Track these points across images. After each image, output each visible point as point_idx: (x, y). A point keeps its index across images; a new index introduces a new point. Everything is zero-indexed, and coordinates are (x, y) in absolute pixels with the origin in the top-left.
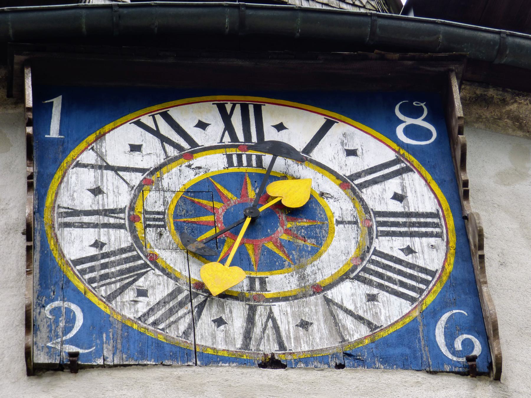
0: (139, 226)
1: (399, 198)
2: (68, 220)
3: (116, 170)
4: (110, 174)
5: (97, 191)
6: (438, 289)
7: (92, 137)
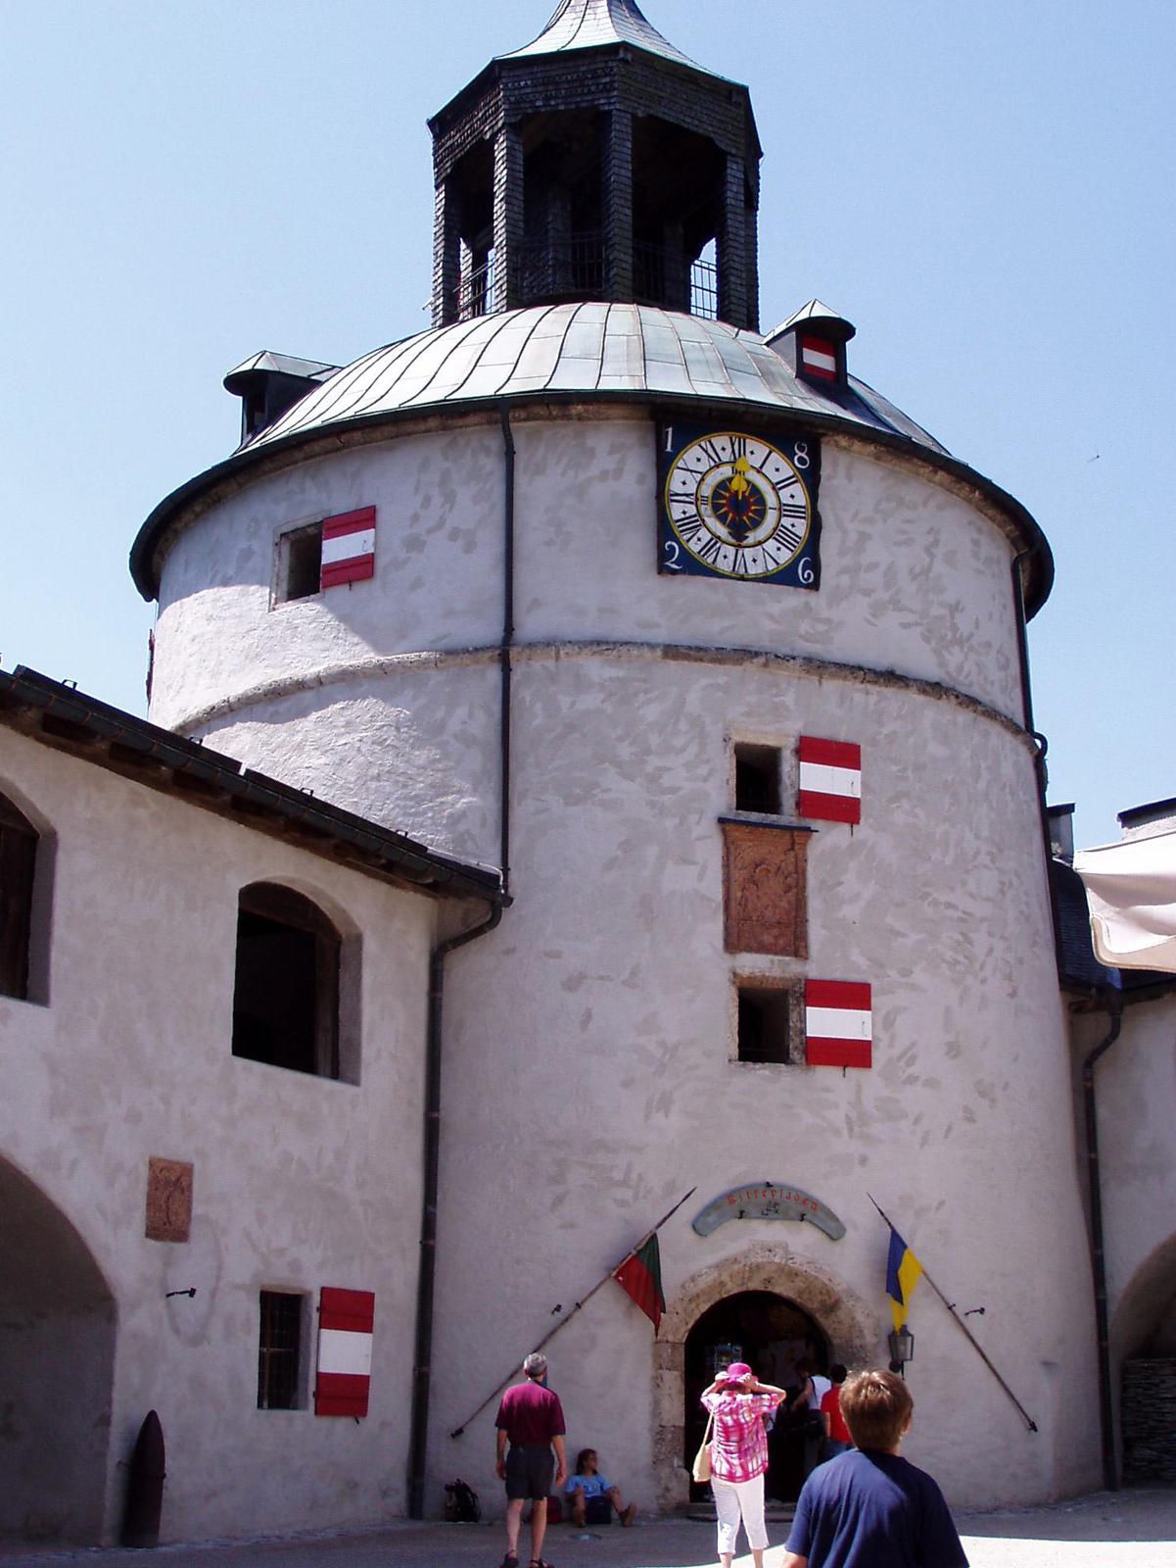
0: (699, 503)
2: (673, 498)
4: (689, 473)
6: (802, 546)
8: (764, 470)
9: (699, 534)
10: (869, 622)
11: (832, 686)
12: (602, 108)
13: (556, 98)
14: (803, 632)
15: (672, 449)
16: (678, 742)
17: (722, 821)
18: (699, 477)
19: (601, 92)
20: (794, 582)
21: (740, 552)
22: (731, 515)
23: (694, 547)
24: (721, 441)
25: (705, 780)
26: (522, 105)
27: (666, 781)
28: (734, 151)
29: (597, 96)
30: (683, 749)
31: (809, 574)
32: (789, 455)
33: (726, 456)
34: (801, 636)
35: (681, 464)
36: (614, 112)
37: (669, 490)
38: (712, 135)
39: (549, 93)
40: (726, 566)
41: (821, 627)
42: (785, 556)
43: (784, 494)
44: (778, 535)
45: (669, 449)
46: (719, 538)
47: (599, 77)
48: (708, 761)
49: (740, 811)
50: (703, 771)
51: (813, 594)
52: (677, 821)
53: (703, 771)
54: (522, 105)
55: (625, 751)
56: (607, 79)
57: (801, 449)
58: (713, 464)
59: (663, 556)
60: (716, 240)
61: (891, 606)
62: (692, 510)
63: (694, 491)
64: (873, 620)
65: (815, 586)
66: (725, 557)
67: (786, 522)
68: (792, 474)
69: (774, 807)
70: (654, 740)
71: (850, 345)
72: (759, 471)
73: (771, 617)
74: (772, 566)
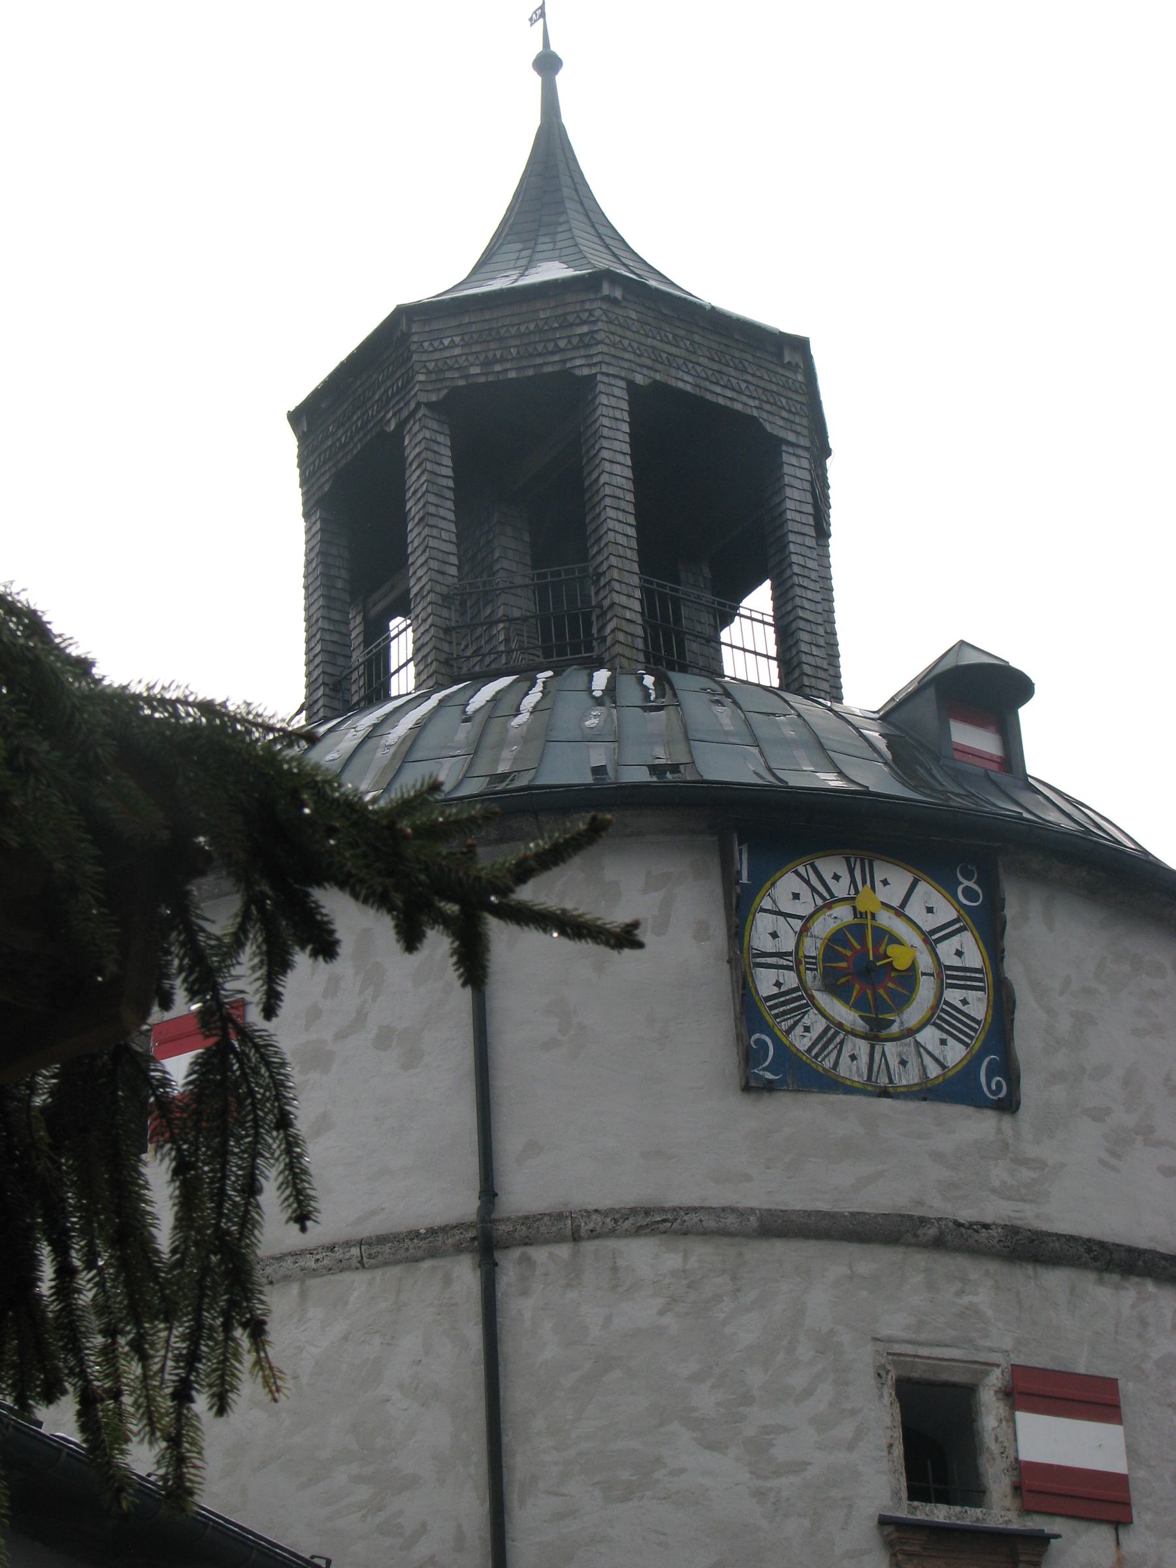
0: (802, 968)
1: (959, 953)
2: (759, 960)
3: (786, 915)
4: (781, 918)
5: (774, 935)
6: (982, 1037)
7: (768, 884)
8: (908, 911)
9: (806, 1021)
10: (1102, 1162)
11: (1056, 1279)
12: (578, 372)
13: (502, 360)
14: (997, 1183)
15: (749, 878)
16: (798, 1379)
17: (884, 1521)
18: (798, 924)
19: (575, 348)
20: (977, 1101)
21: (878, 1049)
22: (857, 987)
23: (801, 1042)
24: (830, 866)
25: (851, 1446)
26: (449, 375)
27: (782, 1451)
28: (791, 437)
29: (569, 355)
30: (808, 1393)
31: (999, 1084)
32: (948, 887)
33: (841, 889)
34: (994, 1191)
35: (767, 903)
36: (599, 377)
37: (750, 948)
38: (755, 413)
39: (490, 355)
40: (851, 1070)
41: (1026, 1174)
42: (955, 1053)
43: (946, 950)
44: (940, 1017)
45: (744, 879)
46: (840, 1025)
47: (571, 325)
48: (853, 1412)
49: (916, 1503)
50: (846, 1430)
51: (1007, 1122)
52: (807, 1523)
53: (846, 1430)
54: (449, 375)
55: (706, 1400)
56: (585, 329)
57: (969, 878)
58: (820, 902)
59: (749, 1057)
60: (774, 588)
61: (1139, 1139)
62: (790, 980)
63: (790, 947)
64: (1113, 1161)
65: (1009, 1105)
66: (853, 1057)
67: (953, 996)
68: (953, 915)
69: (974, 1494)
70: (756, 1378)
71: (1025, 713)
72: (899, 912)
73: (938, 1157)
74: (934, 1071)
